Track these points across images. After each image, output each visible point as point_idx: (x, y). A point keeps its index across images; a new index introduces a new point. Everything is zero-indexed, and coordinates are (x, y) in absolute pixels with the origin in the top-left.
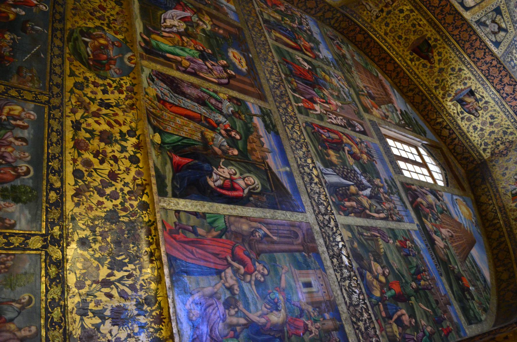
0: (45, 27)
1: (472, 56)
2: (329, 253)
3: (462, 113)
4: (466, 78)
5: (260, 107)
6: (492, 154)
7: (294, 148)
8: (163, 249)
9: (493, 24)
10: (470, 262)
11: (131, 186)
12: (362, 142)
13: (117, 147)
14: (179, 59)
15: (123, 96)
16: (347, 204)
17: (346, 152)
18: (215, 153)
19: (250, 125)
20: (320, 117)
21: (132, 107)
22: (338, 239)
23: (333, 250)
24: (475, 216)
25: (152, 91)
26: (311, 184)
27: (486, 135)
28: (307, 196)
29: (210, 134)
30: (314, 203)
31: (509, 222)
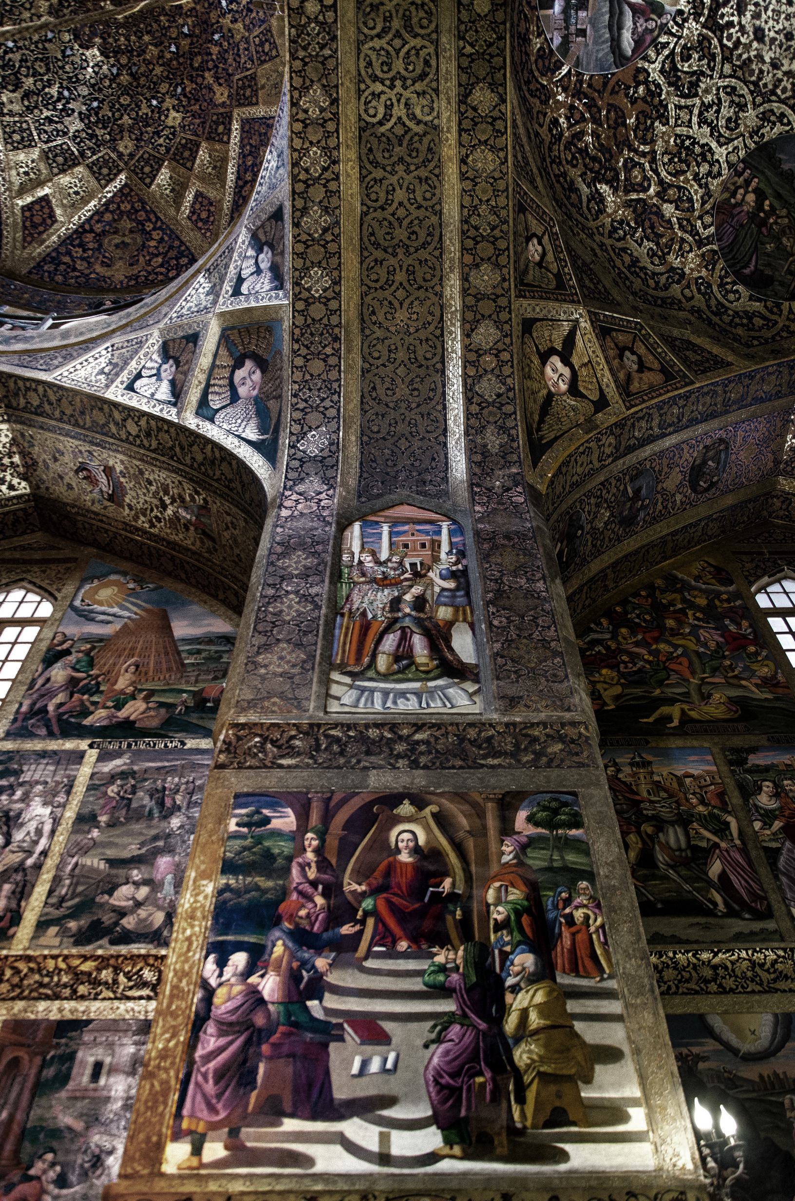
2: (66, 999)
6: (25, 479)
10: (190, 653)
22: (51, 964)
23: (65, 986)
24: (124, 574)
31: (151, 534)
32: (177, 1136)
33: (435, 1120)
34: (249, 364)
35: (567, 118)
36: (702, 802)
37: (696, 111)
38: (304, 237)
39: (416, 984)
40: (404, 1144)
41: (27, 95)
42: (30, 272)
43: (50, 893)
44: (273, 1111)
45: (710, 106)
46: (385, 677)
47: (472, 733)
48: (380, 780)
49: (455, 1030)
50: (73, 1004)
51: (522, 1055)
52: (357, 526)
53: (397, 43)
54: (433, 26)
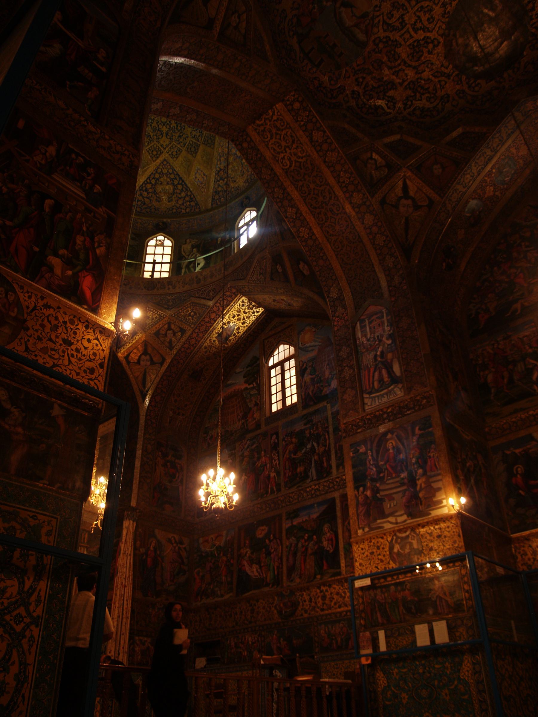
1: (195, 345)
3: (235, 334)
4: (210, 342)
5: (287, 519)
6: (259, 307)
9: (168, 335)
12: (284, 439)
14: (276, 568)
15: (305, 593)
16: (325, 465)
17: (295, 456)
20: (278, 473)
21: (308, 589)
25: (298, 580)
26: (320, 491)
27: (246, 315)
29: (310, 551)
32: (359, 528)
33: (405, 513)
34: (301, 262)
35: (358, 85)
36: (531, 347)
37: (411, 30)
38: (291, 220)
39: (398, 484)
40: (400, 519)
41: (167, 134)
42: (212, 205)
43: (336, 456)
44: (375, 520)
45: (415, 22)
46: (377, 391)
47: (402, 404)
48: (382, 429)
49: (407, 492)
51: (421, 495)
52: (358, 325)
53: (278, 137)
54: (286, 123)
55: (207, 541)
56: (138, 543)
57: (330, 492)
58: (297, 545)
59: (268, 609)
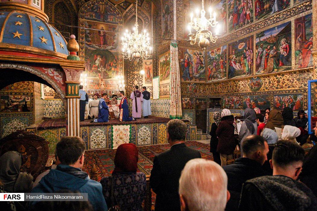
0: (254, 96)
2: (305, 11)
5: (256, 38)
7: (268, 25)
8: (306, 68)
11: (290, 76)
13: (280, 79)
14: (249, 65)
15: (266, 79)
18: (276, 54)
19: (264, 42)
20: (252, 11)
21: (269, 77)
22: (300, 6)
23: (304, 9)
25: (262, 72)
26: (280, 18)
28: (284, 20)
29: (271, 56)
30: (287, 17)
50: (307, 12)
55: (213, 52)
56: (180, 57)
57: (287, 18)
58: (262, 52)
59: (245, 86)
